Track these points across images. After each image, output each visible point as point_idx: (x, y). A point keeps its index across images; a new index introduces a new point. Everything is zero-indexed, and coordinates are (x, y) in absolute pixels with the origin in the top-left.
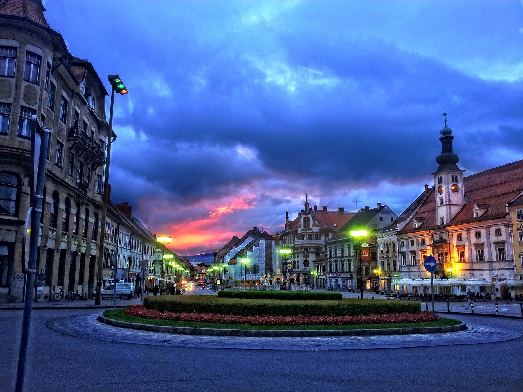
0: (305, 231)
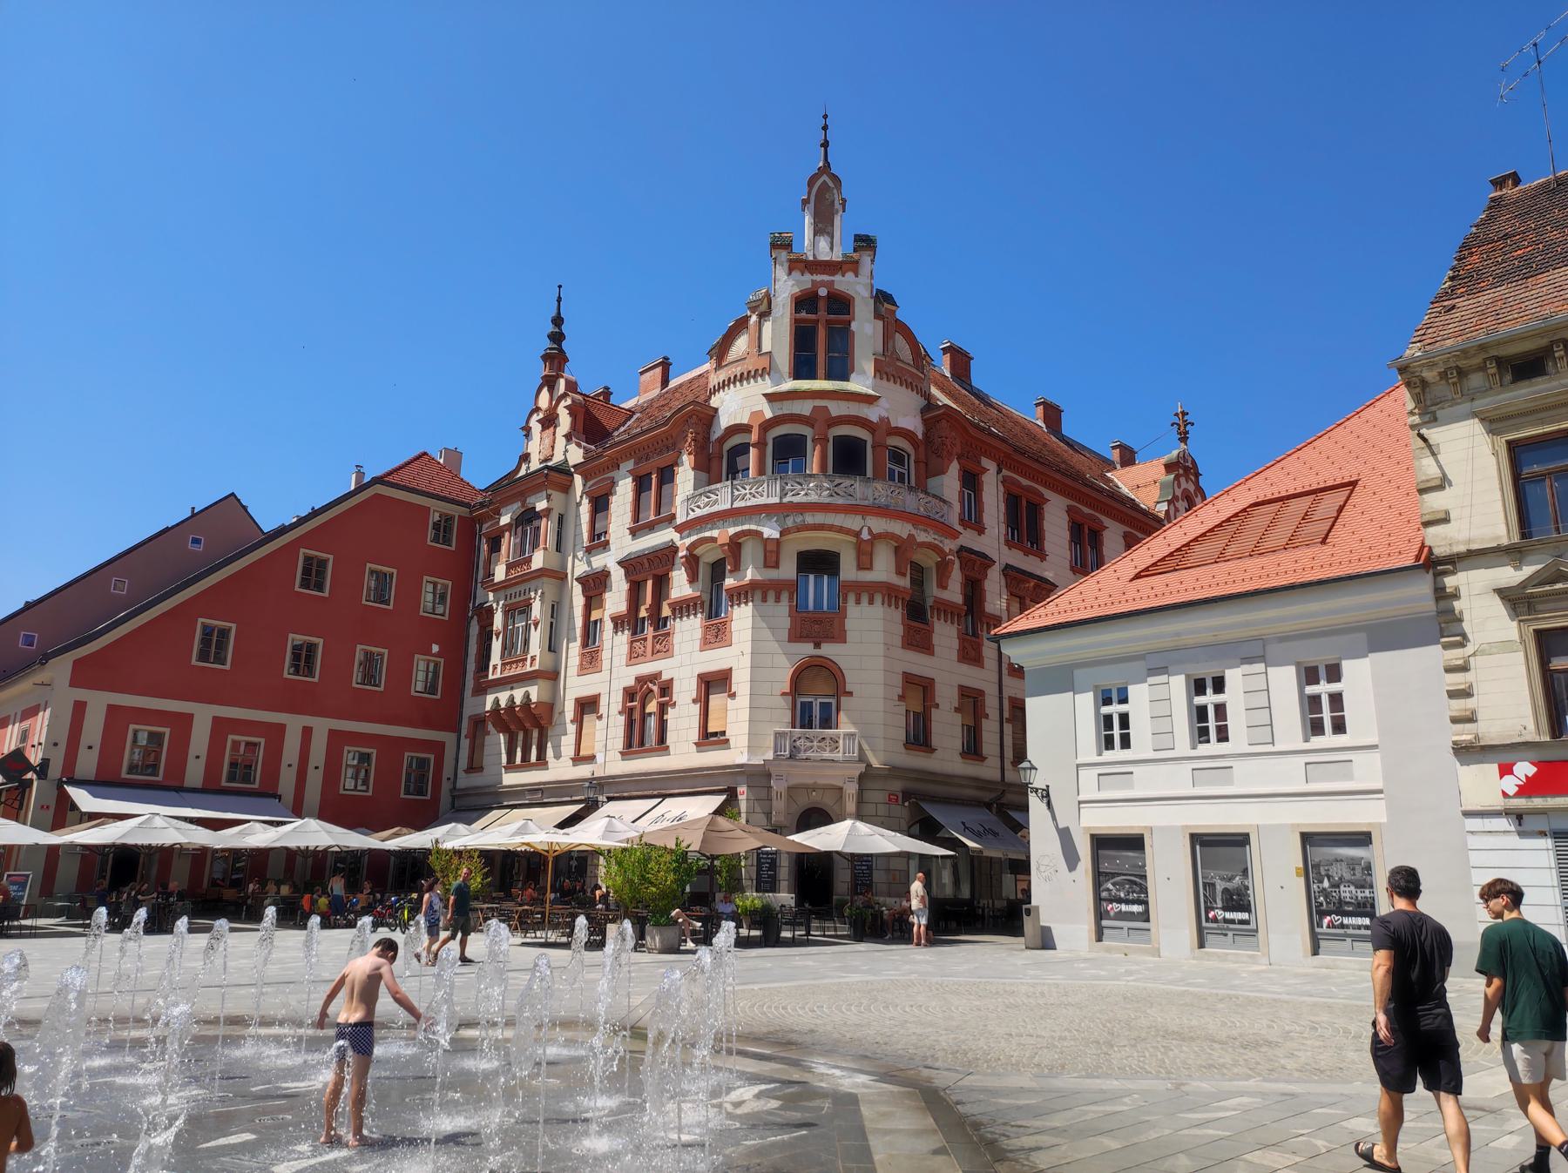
0: (804, 408)
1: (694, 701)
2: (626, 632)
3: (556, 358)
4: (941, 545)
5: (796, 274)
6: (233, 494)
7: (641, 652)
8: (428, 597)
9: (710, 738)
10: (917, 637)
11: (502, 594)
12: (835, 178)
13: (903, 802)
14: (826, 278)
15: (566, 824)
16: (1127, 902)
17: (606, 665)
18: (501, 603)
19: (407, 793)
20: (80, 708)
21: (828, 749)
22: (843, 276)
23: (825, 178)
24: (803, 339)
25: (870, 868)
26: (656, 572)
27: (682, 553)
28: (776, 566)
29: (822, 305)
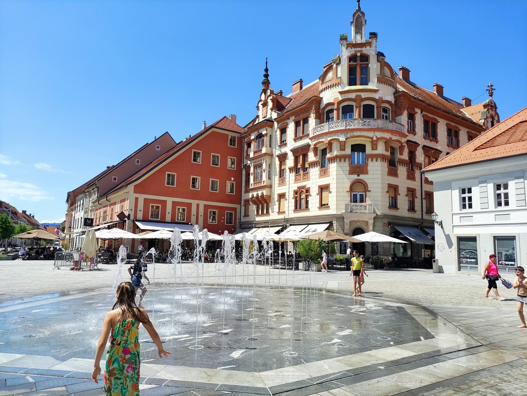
0: (353, 96)
1: (317, 194)
2: (294, 173)
3: (266, 83)
4: (401, 140)
5: (349, 49)
6: (167, 132)
7: (299, 179)
8: (229, 162)
9: (323, 205)
10: (393, 172)
11: (253, 161)
12: (363, 14)
13: (388, 226)
14: (360, 49)
15: (278, 233)
16: (470, 258)
17: (287, 183)
18: (253, 164)
19: (227, 223)
20: (137, 199)
21: (363, 209)
22: (366, 48)
23: (359, 13)
24: (352, 71)
25: (377, 247)
26: (303, 153)
27: (312, 147)
28: (344, 150)
29: (358, 59)
